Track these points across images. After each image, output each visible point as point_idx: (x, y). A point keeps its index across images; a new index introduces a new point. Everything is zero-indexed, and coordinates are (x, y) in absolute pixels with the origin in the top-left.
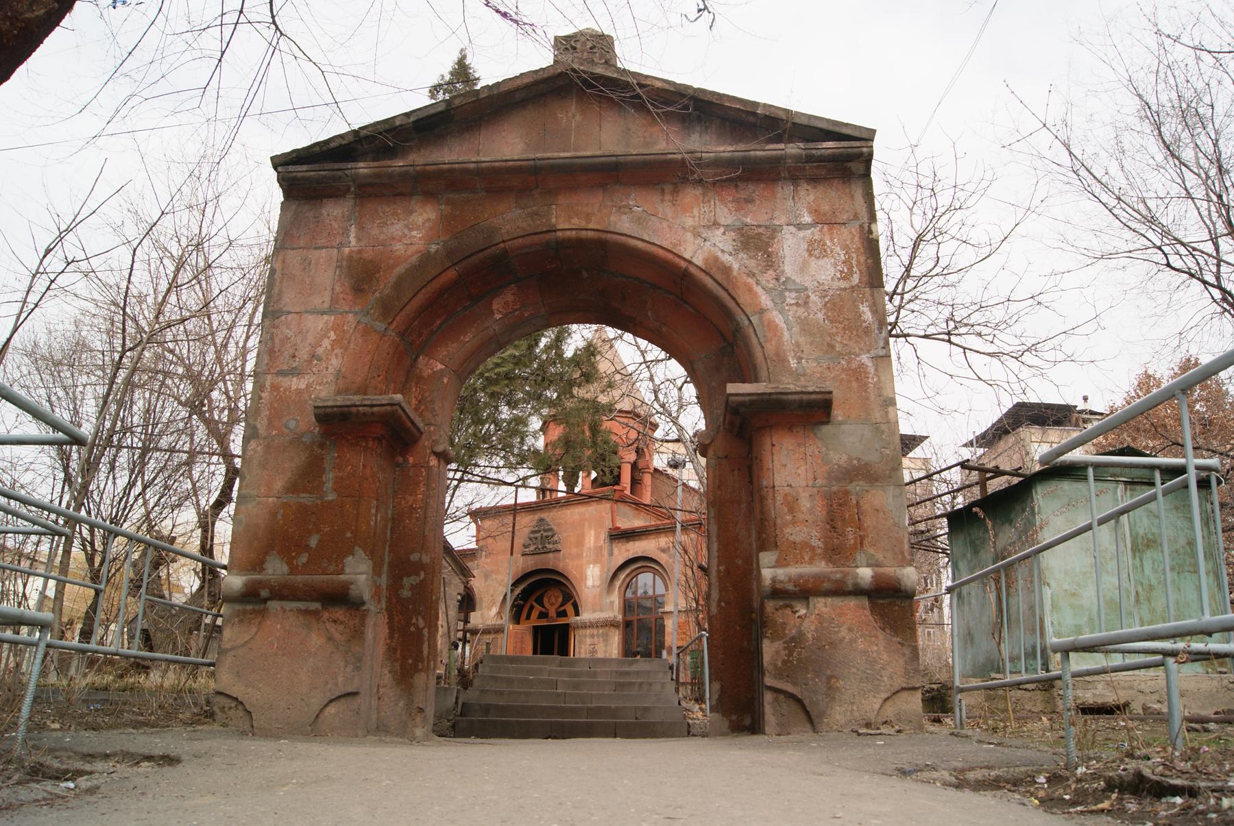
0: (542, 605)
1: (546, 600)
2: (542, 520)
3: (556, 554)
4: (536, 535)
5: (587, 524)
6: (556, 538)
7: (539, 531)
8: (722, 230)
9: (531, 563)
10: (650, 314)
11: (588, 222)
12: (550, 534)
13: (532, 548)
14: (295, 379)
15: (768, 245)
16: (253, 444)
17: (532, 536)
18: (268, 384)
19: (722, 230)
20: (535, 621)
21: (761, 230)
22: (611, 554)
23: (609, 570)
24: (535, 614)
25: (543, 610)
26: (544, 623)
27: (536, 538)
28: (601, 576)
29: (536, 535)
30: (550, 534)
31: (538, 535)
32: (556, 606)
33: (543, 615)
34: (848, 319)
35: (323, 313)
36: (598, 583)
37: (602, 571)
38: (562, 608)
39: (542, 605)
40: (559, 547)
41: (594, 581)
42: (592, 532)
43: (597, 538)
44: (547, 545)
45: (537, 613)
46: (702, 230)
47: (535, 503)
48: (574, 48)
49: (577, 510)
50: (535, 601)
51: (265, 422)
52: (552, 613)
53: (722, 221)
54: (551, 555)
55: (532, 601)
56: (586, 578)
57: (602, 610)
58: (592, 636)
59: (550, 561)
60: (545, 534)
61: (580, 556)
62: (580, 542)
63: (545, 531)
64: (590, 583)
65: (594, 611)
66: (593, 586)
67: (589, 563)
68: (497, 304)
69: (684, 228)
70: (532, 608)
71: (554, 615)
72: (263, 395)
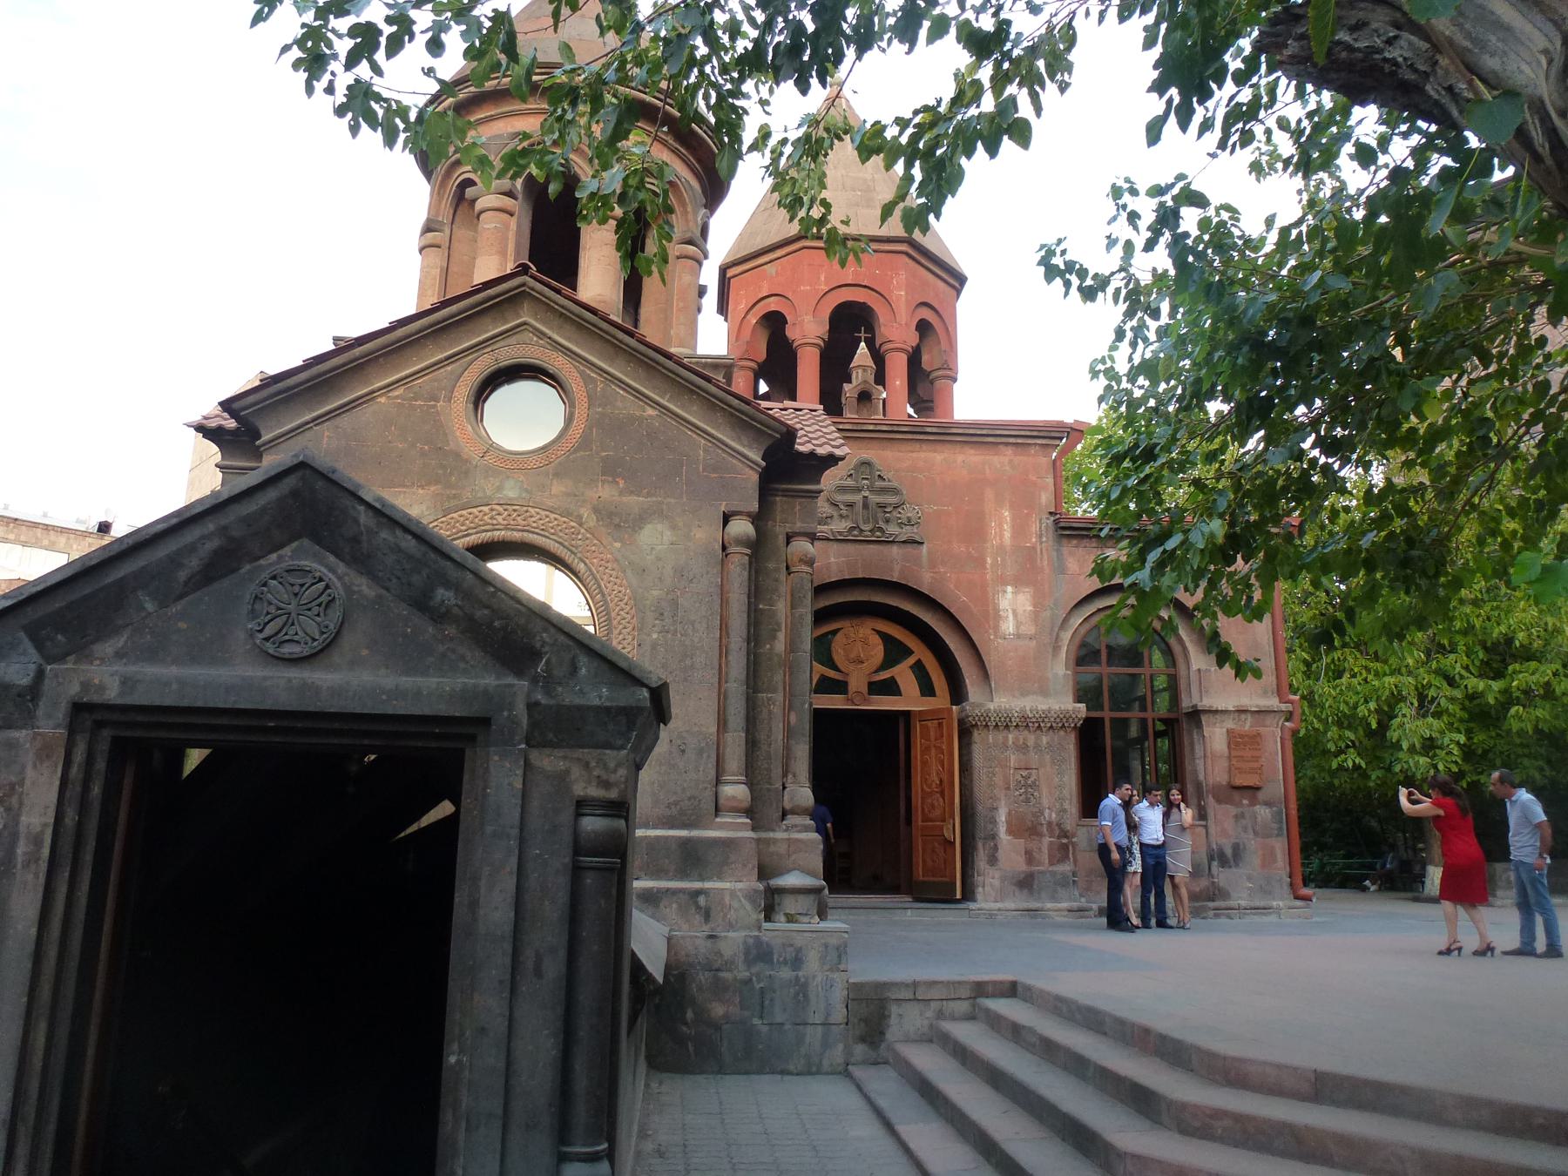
2: (867, 464)
3: (909, 549)
4: (849, 498)
5: (989, 494)
6: (908, 512)
7: (859, 490)
12: (891, 499)
17: (839, 498)
22: (1061, 569)
25: (832, 674)
27: (850, 505)
29: (849, 498)
30: (891, 499)
31: (857, 498)
36: (1029, 629)
37: (1038, 604)
41: (1018, 624)
43: (1019, 529)
49: (960, 458)
52: (857, 682)
54: (895, 549)
56: (997, 616)
57: (1044, 692)
58: (1023, 748)
59: (894, 564)
60: (875, 499)
61: (981, 562)
62: (975, 531)
64: (1009, 626)
65: (1024, 693)
66: (1018, 636)
67: (1004, 582)
71: (865, 689)
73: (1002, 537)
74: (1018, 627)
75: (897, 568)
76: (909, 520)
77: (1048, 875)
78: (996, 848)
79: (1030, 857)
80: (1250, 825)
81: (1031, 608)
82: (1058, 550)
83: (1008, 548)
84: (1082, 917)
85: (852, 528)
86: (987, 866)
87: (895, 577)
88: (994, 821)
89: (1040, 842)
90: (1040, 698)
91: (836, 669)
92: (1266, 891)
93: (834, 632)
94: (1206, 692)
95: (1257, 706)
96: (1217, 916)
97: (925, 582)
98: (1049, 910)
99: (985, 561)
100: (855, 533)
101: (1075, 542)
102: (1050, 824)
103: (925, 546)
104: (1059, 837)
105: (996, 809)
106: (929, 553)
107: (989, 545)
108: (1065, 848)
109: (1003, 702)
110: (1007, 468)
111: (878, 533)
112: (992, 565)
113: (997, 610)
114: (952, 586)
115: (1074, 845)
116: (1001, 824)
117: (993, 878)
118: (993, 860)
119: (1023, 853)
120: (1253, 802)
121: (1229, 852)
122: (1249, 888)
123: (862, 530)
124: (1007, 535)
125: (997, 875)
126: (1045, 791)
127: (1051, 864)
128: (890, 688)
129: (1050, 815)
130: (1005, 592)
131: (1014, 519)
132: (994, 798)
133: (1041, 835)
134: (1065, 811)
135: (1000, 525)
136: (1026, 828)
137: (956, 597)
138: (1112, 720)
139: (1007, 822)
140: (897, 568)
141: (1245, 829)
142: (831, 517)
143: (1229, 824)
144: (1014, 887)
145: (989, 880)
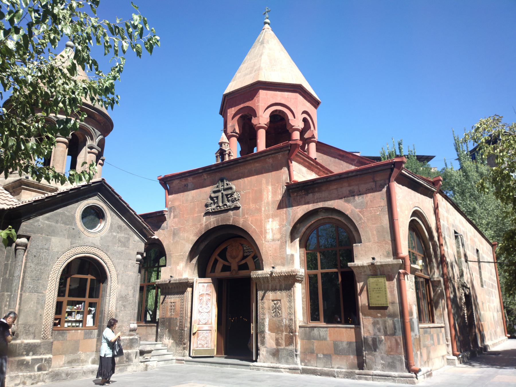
0: (226, 260)
4: (216, 195)
6: (235, 196)
7: (219, 191)
9: (213, 221)
12: (229, 192)
13: (213, 207)
20: (218, 273)
24: (219, 267)
25: (226, 263)
26: (227, 274)
28: (280, 229)
30: (229, 192)
31: (220, 194)
32: (237, 260)
33: (226, 268)
36: (278, 236)
37: (281, 225)
38: (243, 262)
40: (238, 204)
41: (274, 234)
42: (270, 188)
43: (274, 193)
44: (228, 204)
47: (215, 165)
50: (219, 255)
52: (234, 266)
54: (231, 213)
55: (215, 256)
56: (266, 232)
59: (231, 218)
60: (225, 193)
61: (259, 210)
63: (225, 190)
64: (269, 236)
66: (273, 240)
67: (268, 217)
70: (216, 261)
73: (268, 199)
74: (273, 236)
75: (232, 219)
76: (235, 199)
77: (285, 351)
78: (264, 337)
79: (278, 343)
80: (382, 328)
81: (278, 227)
82: (289, 199)
83: (270, 202)
84: (295, 373)
85: (217, 206)
86: (261, 346)
87: (231, 222)
88: (264, 325)
89: (282, 334)
90: (282, 267)
91: (228, 261)
92: (392, 366)
94: (356, 257)
95: (380, 262)
96: (360, 378)
97: (240, 223)
98: (281, 368)
99: (262, 210)
100: (218, 208)
101: (295, 194)
102: (286, 325)
103: (241, 209)
104: (289, 333)
105: (264, 319)
106: (242, 210)
107: (263, 203)
110: (271, 168)
111: (225, 207)
112: (264, 210)
113: (265, 230)
114: (250, 223)
115: (295, 335)
116: (266, 326)
117: (263, 351)
118: (263, 343)
119: (275, 339)
120: (383, 315)
121: (370, 342)
122: (382, 364)
123: (220, 207)
124: (270, 196)
125: (265, 349)
126: (283, 309)
127: (286, 346)
128: (245, 267)
129: (286, 322)
130: (269, 221)
131: (272, 189)
132: (264, 314)
133: (282, 331)
134: (291, 320)
135: (268, 193)
136: (276, 328)
137: (252, 228)
139: (269, 325)
140: (232, 219)
141: (379, 330)
142: (212, 203)
143: (370, 328)
144: (271, 356)
145: (263, 351)
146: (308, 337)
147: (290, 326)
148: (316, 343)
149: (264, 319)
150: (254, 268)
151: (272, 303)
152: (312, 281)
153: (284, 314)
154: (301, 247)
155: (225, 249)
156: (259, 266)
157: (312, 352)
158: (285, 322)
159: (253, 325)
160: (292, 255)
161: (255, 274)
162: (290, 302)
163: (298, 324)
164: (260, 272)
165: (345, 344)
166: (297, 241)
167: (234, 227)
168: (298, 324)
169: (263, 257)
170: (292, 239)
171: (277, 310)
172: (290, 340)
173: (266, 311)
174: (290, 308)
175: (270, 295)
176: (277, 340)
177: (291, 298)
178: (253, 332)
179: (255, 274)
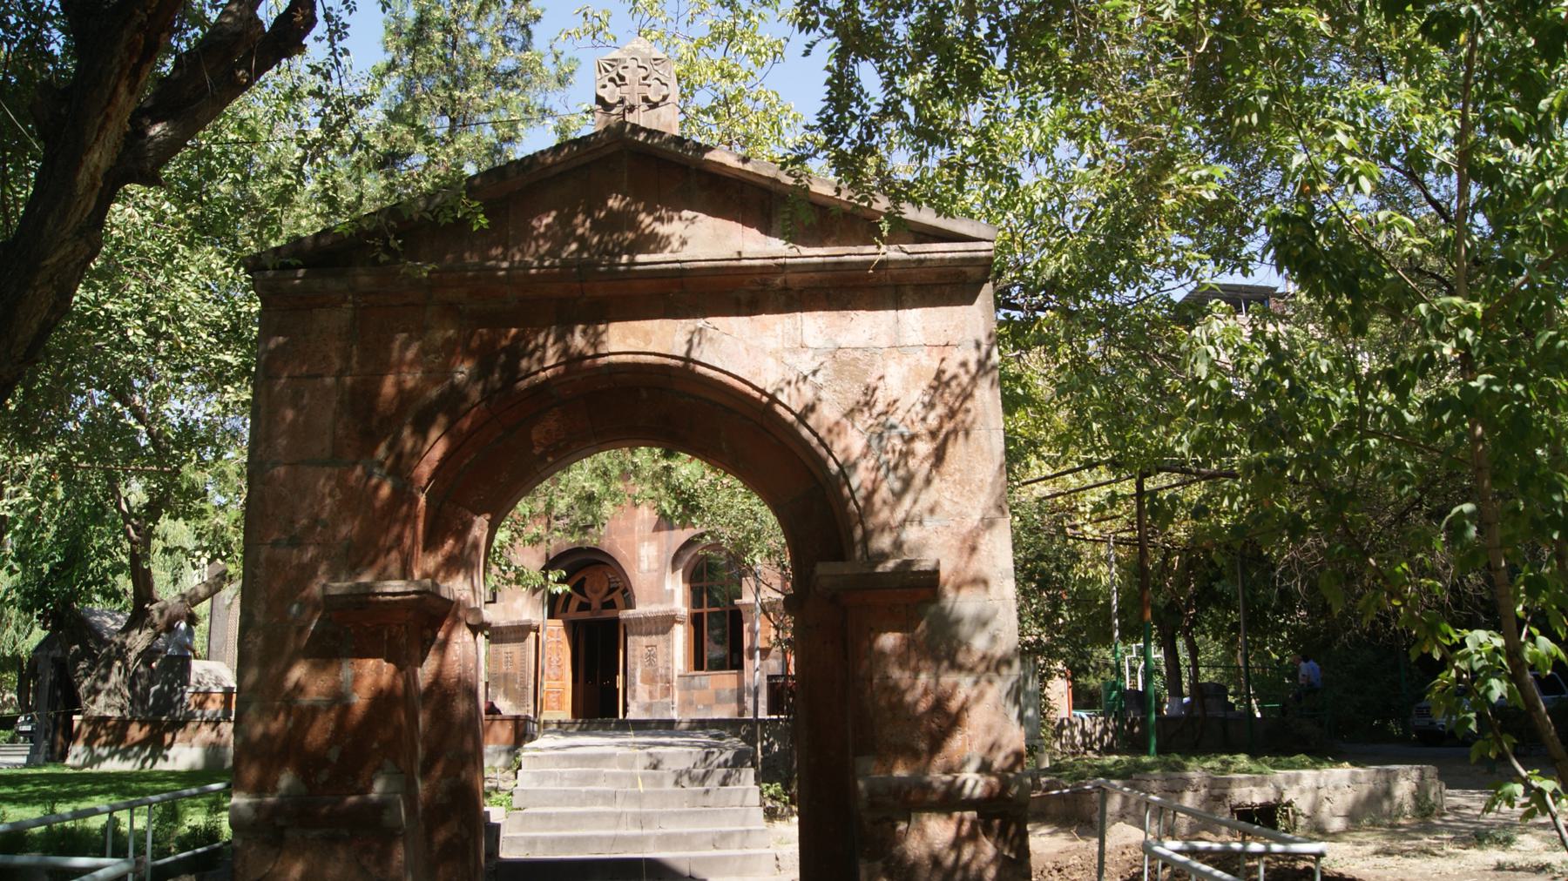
0: (584, 595)
1: (587, 590)
8: (811, 353)
10: (724, 445)
11: (648, 342)
14: (295, 551)
15: (865, 372)
16: (251, 636)
18: (262, 557)
19: (811, 353)
21: (858, 354)
23: (669, 549)
24: (574, 604)
25: (584, 600)
26: (585, 615)
32: (601, 595)
33: (583, 607)
34: (960, 470)
35: (324, 464)
36: (655, 566)
38: (609, 598)
39: (584, 595)
41: (649, 563)
45: (577, 604)
46: (786, 355)
48: (622, 78)
51: (263, 606)
52: (596, 604)
53: (810, 342)
56: (639, 560)
57: (661, 602)
59: (591, 540)
61: (632, 530)
64: (644, 566)
65: (652, 603)
66: (649, 571)
67: (642, 540)
68: (536, 434)
69: (763, 351)
72: (257, 571)
79: (651, 695)
93: (584, 579)
97: (606, 546)
108: (668, 689)
109: (642, 609)
118: (633, 697)
128: (611, 605)
132: (635, 663)
136: (650, 679)
137: (621, 553)
138: (702, 614)
146: (687, 688)
147: (666, 676)
148: (696, 694)
149: (635, 669)
150: (623, 605)
151: (646, 650)
152: (696, 621)
153: (660, 662)
154: (684, 582)
155: (584, 579)
156: (630, 604)
157: (691, 703)
158: (662, 671)
159: (620, 678)
160: (672, 591)
161: (625, 614)
162: (668, 647)
163: (676, 674)
164: (631, 612)
165: (727, 693)
166: (680, 572)
167: (595, 551)
168: (676, 674)
169: (636, 592)
170: (674, 569)
171: (651, 657)
172: (667, 691)
173: (638, 661)
174: (668, 654)
175: (645, 640)
176: (650, 692)
177: (669, 644)
178: (620, 685)
179: (625, 614)
